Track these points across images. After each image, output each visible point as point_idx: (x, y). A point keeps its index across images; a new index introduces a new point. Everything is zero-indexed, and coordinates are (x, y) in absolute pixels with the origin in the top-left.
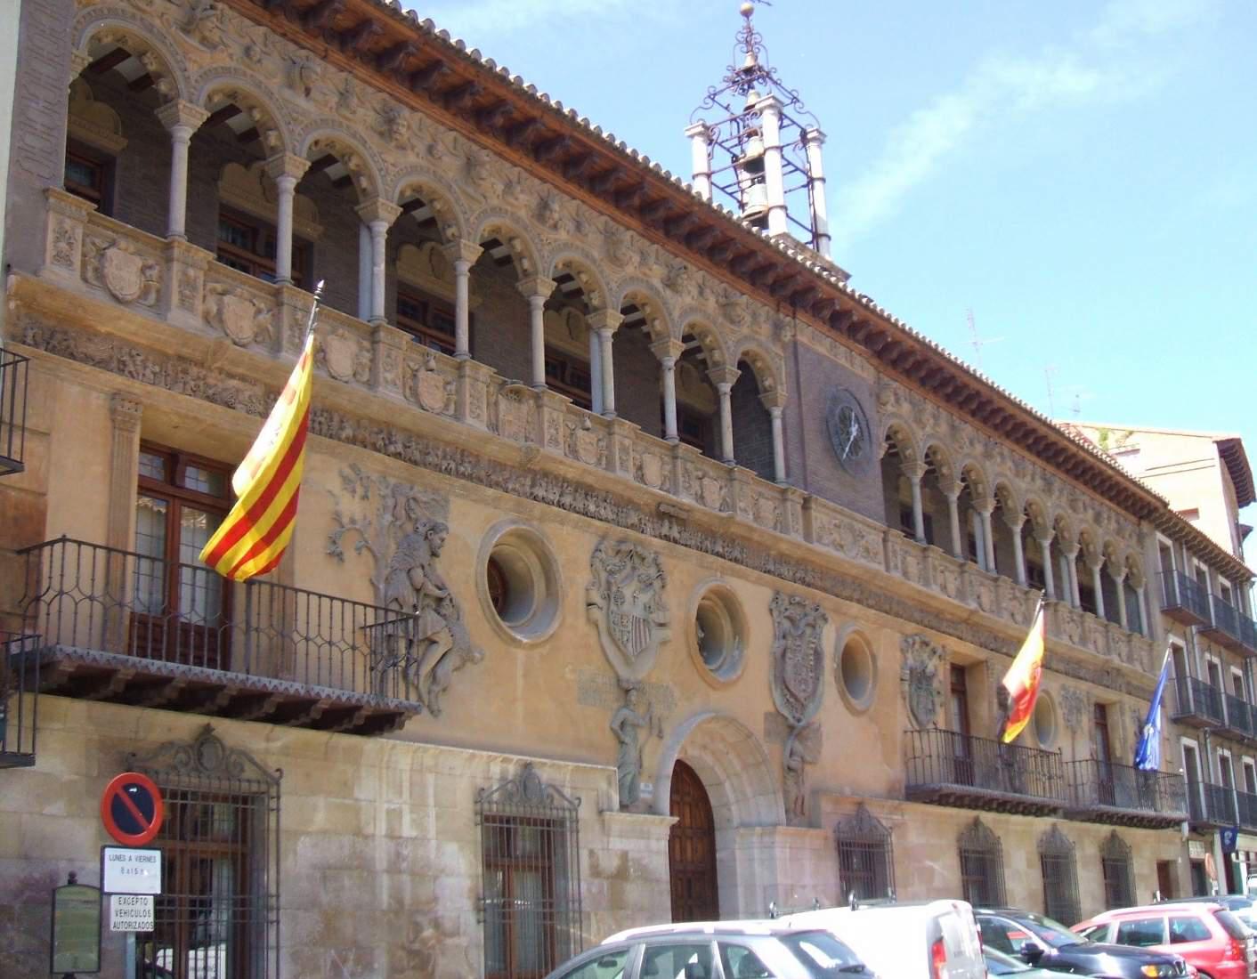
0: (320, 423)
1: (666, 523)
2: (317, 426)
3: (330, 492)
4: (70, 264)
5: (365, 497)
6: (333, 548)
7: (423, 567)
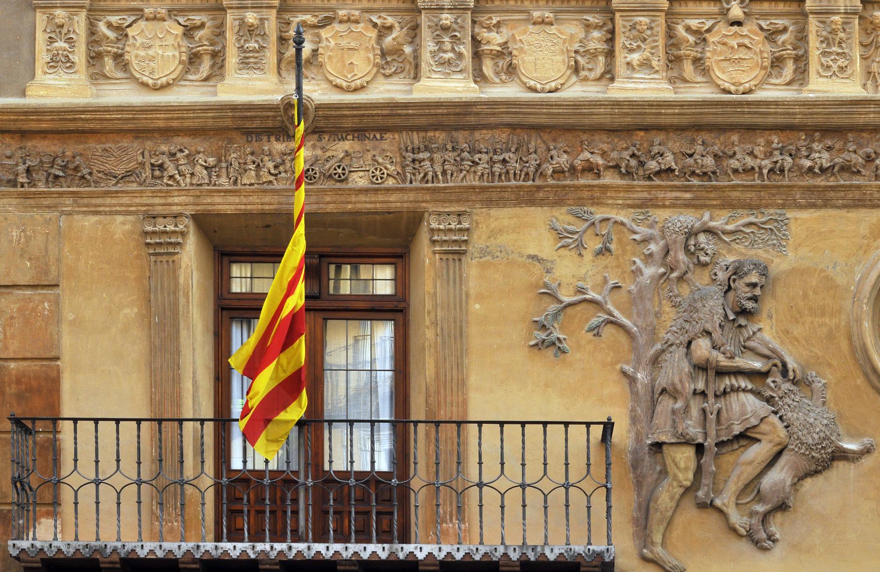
0: (504, 161)
2: (497, 168)
3: (533, 257)
4: (70, 65)
5: (605, 251)
6: (543, 335)
7: (709, 333)
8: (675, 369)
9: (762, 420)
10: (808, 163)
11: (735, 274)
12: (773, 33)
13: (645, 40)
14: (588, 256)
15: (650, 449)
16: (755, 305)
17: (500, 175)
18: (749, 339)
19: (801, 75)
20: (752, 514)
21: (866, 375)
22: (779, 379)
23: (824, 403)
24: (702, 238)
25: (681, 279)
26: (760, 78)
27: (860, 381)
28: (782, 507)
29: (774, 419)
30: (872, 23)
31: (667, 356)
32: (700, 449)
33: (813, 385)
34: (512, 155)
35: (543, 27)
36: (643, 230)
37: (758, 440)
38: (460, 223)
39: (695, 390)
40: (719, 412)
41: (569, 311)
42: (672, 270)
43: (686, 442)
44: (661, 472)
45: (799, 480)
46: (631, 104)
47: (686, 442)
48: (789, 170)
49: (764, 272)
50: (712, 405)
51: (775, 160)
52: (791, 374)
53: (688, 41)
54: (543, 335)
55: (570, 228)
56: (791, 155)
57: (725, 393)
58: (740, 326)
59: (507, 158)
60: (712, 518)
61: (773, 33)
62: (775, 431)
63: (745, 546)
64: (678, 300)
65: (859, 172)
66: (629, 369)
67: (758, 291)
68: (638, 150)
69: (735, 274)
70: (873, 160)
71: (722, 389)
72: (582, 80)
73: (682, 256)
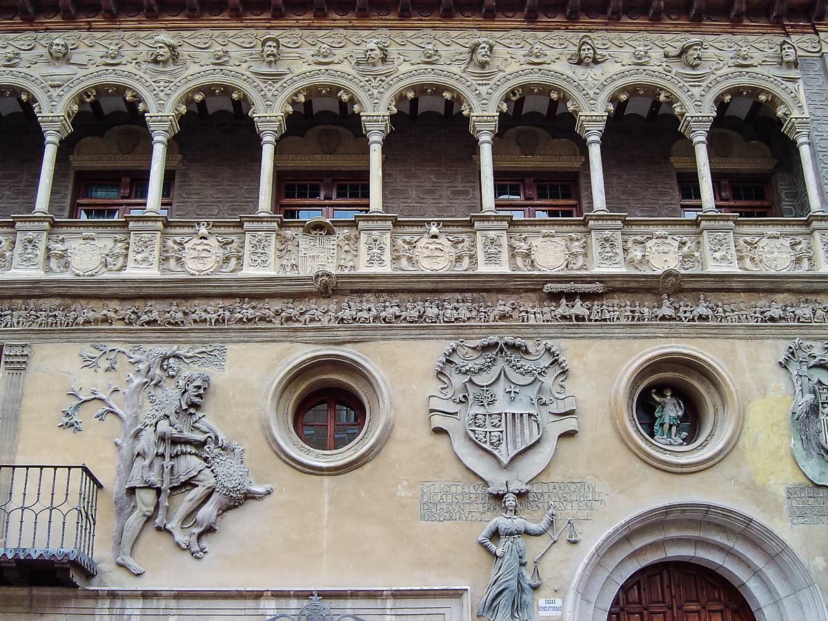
1: (564, 301)
5: (111, 369)
6: (66, 420)
8: (148, 440)
9: (199, 472)
10: (240, 316)
11: (189, 381)
12: (226, 244)
13: (147, 247)
14: (101, 371)
15: (127, 492)
16: (200, 400)
17: (52, 324)
18: (196, 422)
19: (240, 265)
20: (192, 534)
21: (269, 443)
22: (212, 446)
23: (242, 461)
24: (172, 360)
25: (156, 385)
26: (214, 268)
27: (266, 448)
28: (210, 530)
29: (208, 471)
30: (284, 237)
31: (143, 433)
32: (159, 491)
33: (235, 451)
34: (60, 312)
35: (88, 241)
36: (137, 357)
37: (198, 486)
38: (23, 351)
39: (157, 453)
40: (173, 467)
41: (85, 404)
42: (152, 380)
43: (150, 487)
44: (134, 507)
45: (223, 512)
46: (133, 281)
47: (150, 487)
48: (228, 321)
49: (206, 380)
50: (168, 462)
51: (219, 314)
52: (220, 442)
53: (173, 248)
54: (66, 420)
55: (91, 355)
56: (230, 311)
57: (177, 456)
58: (191, 414)
59: (57, 314)
60: (164, 537)
61: (226, 244)
62: (207, 480)
63: (187, 555)
64: (154, 398)
65: (271, 321)
66: (119, 441)
67: (202, 391)
68: (137, 309)
69: (189, 381)
70: (280, 315)
71: (175, 452)
72: (109, 270)
73: (158, 371)
